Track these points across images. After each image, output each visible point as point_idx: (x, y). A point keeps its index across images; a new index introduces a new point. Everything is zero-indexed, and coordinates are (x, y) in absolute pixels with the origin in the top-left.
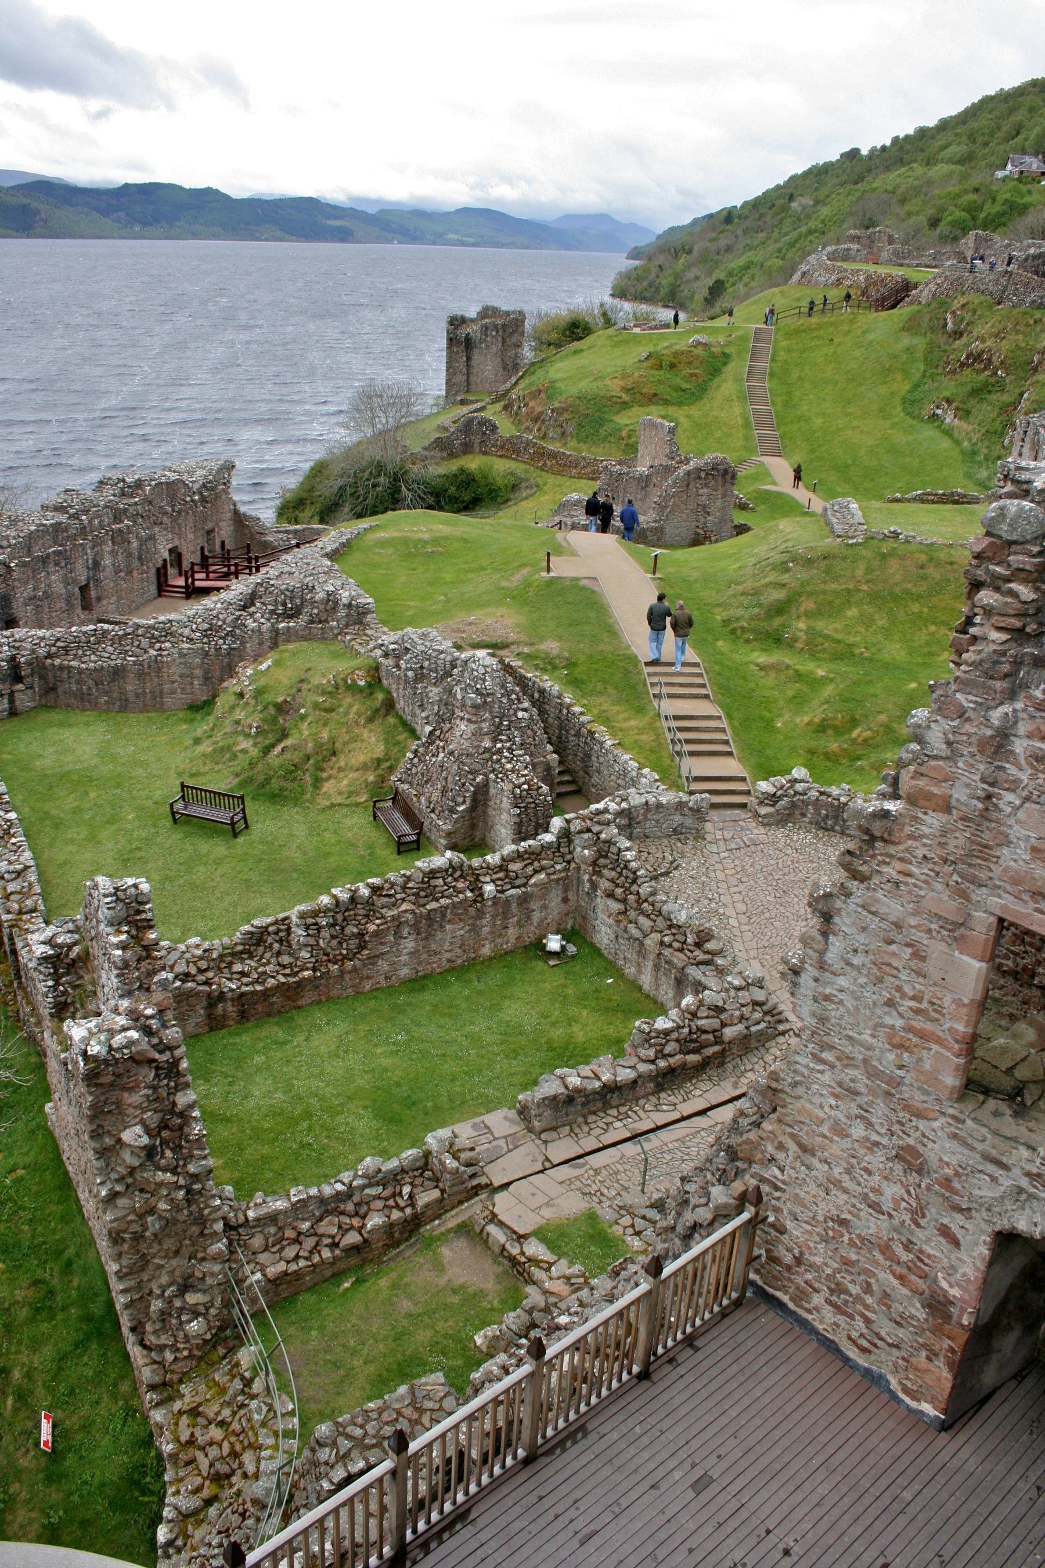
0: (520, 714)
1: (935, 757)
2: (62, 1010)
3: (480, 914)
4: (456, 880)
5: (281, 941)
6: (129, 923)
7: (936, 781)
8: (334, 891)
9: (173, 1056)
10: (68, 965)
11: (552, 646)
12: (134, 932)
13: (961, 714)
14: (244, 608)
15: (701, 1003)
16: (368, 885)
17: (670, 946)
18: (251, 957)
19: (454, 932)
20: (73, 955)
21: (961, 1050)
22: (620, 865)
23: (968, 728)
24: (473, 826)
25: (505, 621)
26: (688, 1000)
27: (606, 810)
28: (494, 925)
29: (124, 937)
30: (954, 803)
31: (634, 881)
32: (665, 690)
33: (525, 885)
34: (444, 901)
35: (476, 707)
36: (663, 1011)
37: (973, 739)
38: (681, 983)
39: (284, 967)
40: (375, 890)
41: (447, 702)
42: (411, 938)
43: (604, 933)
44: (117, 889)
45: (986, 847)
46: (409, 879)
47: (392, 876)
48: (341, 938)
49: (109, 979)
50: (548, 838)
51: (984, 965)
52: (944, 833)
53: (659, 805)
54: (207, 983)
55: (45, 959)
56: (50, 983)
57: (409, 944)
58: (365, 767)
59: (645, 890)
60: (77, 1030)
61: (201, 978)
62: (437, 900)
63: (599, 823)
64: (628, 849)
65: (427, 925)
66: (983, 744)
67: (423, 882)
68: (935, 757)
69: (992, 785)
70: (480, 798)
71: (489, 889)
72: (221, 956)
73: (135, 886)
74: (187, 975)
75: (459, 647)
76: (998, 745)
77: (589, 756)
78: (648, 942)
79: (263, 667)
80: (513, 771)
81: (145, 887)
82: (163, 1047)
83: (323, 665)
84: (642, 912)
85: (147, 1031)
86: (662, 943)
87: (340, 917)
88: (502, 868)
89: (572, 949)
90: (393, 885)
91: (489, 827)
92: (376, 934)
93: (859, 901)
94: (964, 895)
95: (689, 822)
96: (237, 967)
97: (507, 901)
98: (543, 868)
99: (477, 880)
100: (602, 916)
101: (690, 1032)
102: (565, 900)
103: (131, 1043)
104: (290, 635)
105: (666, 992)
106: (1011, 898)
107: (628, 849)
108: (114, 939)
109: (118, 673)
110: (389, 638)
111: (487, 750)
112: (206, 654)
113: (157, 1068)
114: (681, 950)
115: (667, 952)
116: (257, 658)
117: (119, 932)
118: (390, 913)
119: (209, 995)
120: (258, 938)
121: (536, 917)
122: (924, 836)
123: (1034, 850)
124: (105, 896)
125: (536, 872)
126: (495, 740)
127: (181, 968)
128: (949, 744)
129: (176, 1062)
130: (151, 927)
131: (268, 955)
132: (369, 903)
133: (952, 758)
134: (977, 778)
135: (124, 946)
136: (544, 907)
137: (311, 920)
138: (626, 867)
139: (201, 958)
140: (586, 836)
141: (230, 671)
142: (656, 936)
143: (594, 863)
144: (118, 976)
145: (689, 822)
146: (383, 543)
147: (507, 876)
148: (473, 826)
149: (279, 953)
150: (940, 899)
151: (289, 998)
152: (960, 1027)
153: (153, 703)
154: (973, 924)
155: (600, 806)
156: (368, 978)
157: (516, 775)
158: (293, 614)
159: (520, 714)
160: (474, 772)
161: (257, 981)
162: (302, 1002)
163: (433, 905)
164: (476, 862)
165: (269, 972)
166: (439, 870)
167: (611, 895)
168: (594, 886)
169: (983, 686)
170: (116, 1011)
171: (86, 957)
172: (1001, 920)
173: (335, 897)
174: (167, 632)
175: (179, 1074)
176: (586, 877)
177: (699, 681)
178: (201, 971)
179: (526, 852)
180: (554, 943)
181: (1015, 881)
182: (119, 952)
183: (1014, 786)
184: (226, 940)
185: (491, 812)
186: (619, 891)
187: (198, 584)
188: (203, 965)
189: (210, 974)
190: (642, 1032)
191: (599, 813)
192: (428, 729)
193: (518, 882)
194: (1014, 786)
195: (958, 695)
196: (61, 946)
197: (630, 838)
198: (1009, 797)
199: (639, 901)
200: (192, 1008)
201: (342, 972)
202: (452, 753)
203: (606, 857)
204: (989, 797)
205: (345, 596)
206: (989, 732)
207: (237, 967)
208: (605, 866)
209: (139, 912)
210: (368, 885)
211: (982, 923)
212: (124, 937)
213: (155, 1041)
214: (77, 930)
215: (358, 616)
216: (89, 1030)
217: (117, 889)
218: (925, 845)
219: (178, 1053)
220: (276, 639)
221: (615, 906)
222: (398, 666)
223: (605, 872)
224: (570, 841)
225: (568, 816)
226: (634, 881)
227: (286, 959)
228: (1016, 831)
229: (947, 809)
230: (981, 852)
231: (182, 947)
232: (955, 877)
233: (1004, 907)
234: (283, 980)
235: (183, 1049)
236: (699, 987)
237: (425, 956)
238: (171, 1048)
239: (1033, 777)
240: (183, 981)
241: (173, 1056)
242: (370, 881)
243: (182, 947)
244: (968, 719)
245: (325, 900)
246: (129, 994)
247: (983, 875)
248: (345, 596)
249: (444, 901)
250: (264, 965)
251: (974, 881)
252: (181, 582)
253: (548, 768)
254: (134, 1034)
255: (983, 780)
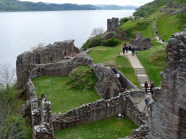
0: (114, 76)
1: (165, 80)
2: (36, 124)
3: (107, 110)
4: (103, 103)
5: (74, 114)
6: (47, 109)
7: (166, 84)
8: (83, 105)
9: (51, 133)
10: (38, 116)
11: (120, 66)
12: (47, 111)
13: (168, 72)
14: (73, 61)
15: (144, 127)
16: (88, 104)
17: (139, 116)
18: (69, 116)
19: (103, 113)
20: (38, 114)
21: (177, 134)
22: (130, 101)
23: (169, 74)
24: (107, 95)
25: (112, 62)
26: (142, 126)
27: (128, 92)
28: (109, 112)
29: (45, 111)
30: (169, 87)
31: (133, 104)
32: (138, 73)
33: (114, 105)
34: (101, 107)
35: (107, 75)
36: (138, 128)
37: (170, 76)
38: (142, 123)
39: (74, 118)
40: (90, 105)
41: (103, 75)
42: (96, 113)
43: (128, 114)
44: (45, 103)
45: (175, 95)
46: (95, 103)
47: (92, 103)
48: (84, 113)
49: (43, 119)
50: (118, 97)
51: (178, 117)
52: (168, 92)
53: (137, 91)
54: (61, 120)
55: (34, 115)
56: (34, 119)
57: (95, 115)
58: (90, 86)
59: (135, 106)
60: (36, 127)
61: (60, 120)
62: (100, 107)
63: (127, 94)
64: (131, 99)
65: (98, 111)
66: (172, 77)
67: (97, 104)
68: (165, 80)
69: (174, 84)
70: (108, 90)
71: (108, 105)
72: (64, 116)
73: (48, 103)
74: (58, 119)
75: (105, 67)
76: (174, 77)
77: (126, 83)
78: (135, 115)
79: (76, 69)
80: (113, 86)
81: (50, 103)
82: (50, 131)
83: (85, 69)
84: (134, 110)
85: (48, 128)
86: (138, 115)
87: (84, 110)
88: (111, 102)
89: (123, 116)
90: (93, 104)
91: (110, 95)
92: (90, 113)
93: (156, 105)
94: (173, 104)
95: (142, 94)
96: (66, 118)
97: (112, 108)
98: (118, 102)
99: (107, 104)
100: (128, 110)
101: (142, 132)
102: (122, 107)
103: (44, 130)
104: (80, 65)
105: (139, 124)
106: (181, 104)
107: (131, 99)
108: (44, 112)
109: (54, 71)
110: (95, 65)
111: (109, 82)
112: (68, 68)
113: (49, 135)
114: (141, 117)
115: (139, 117)
116: (75, 68)
117: (45, 111)
118: (91, 109)
119: (61, 122)
120: (70, 113)
121: (117, 110)
122: (164, 93)
123: (183, 95)
124: (43, 104)
125: (116, 102)
126: (110, 81)
127: (57, 118)
128: (166, 77)
129: (52, 134)
130: (50, 110)
131: (72, 116)
132: (88, 107)
133: (167, 79)
134: (172, 83)
135: (45, 113)
136: (118, 109)
137: (79, 110)
138: (131, 102)
139: (61, 116)
140: (124, 96)
141: (71, 70)
142: (137, 114)
143: (126, 101)
144: (44, 118)
145: (142, 94)
146: (95, 51)
147: (112, 103)
148: (107, 95)
149: (74, 116)
150: (168, 104)
151: (75, 124)
152: (176, 129)
153: (59, 75)
154: (176, 109)
155: (127, 91)
156: (88, 120)
157: (114, 86)
158: (80, 62)
159: (114, 76)
160: (107, 86)
161: (69, 121)
162: (77, 124)
163: (99, 108)
164: (106, 101)
165: (72, 119)
166: (100, 102)
167: (129, 107)
168: (126, 105)
169: (170, 67)
170: (43, 124)
171: (40, 115)
172: (180, 108)
173: (83, 106)
174: (62, 64)
175: (52, 136)
176: (125, 104)
177: (143, 71)
178: (60, 118)
179: (115, 99)
180: (120, 115)
181: (181, 101)
182: (44, 114)
183: (178, 84)
184: (65, 113)
185: (110, 92)
186: (130, 106)
187: (68, 57)
188: (61, 117)
189: (62, 119)
190: (134, 131)
191: (126, 92)
192: (100, 79)
193: (113, 104)
194: (178, 84)
195: (167, 69)
196: (36, 113)
197: (132, 97)
198: (178, 86)
199: (134, 108)
200: (58, 125)
201: (84, 119)
202: (104, 83)
203: (128, 100)
204: (174, 86)
205: (88, 59)
206: (173, 75)
207: (66, 118)
208: (128, 102)
209: (49, 107)
210: (88, 104)
211: (177, 109)
212: (45, 111)
213: (49, 130)
214: (39, 110)
215: (90, 62)
216: (38, 127)
217: (45, 103)
218: (165, 95)
219: (52, 132)
220: (78, 65)
221: (130, 109)
222: (96, 69)
223: (128, 103)
224: (122, 97)
225: (122, 93)
226: (133, 104)
227: (74, 117)
228: (180, 92)
229: (168, 88)
230: (174, 96)
231: (58, 114)
232: (171, 100)
233: (180, 106)
234: (74, 120)
235: (53, 131)
236: (144, 123)
237: (98, 117)
238: (51, 131)
239: (181, 83)
240: (57, 120)
241: (51, 133)
242: (89, 103)
243: (58, 114)
244: (169, 73)
245: (81, 106)
246: (46, 121)
247: (176, 100)
248: (88, 59)
249: (101, 107)
250: (71, 118)
251: (174, 101)
252: (66, 57)
253: (119, 85)
254: (45, 128)
255: (173, 83)
